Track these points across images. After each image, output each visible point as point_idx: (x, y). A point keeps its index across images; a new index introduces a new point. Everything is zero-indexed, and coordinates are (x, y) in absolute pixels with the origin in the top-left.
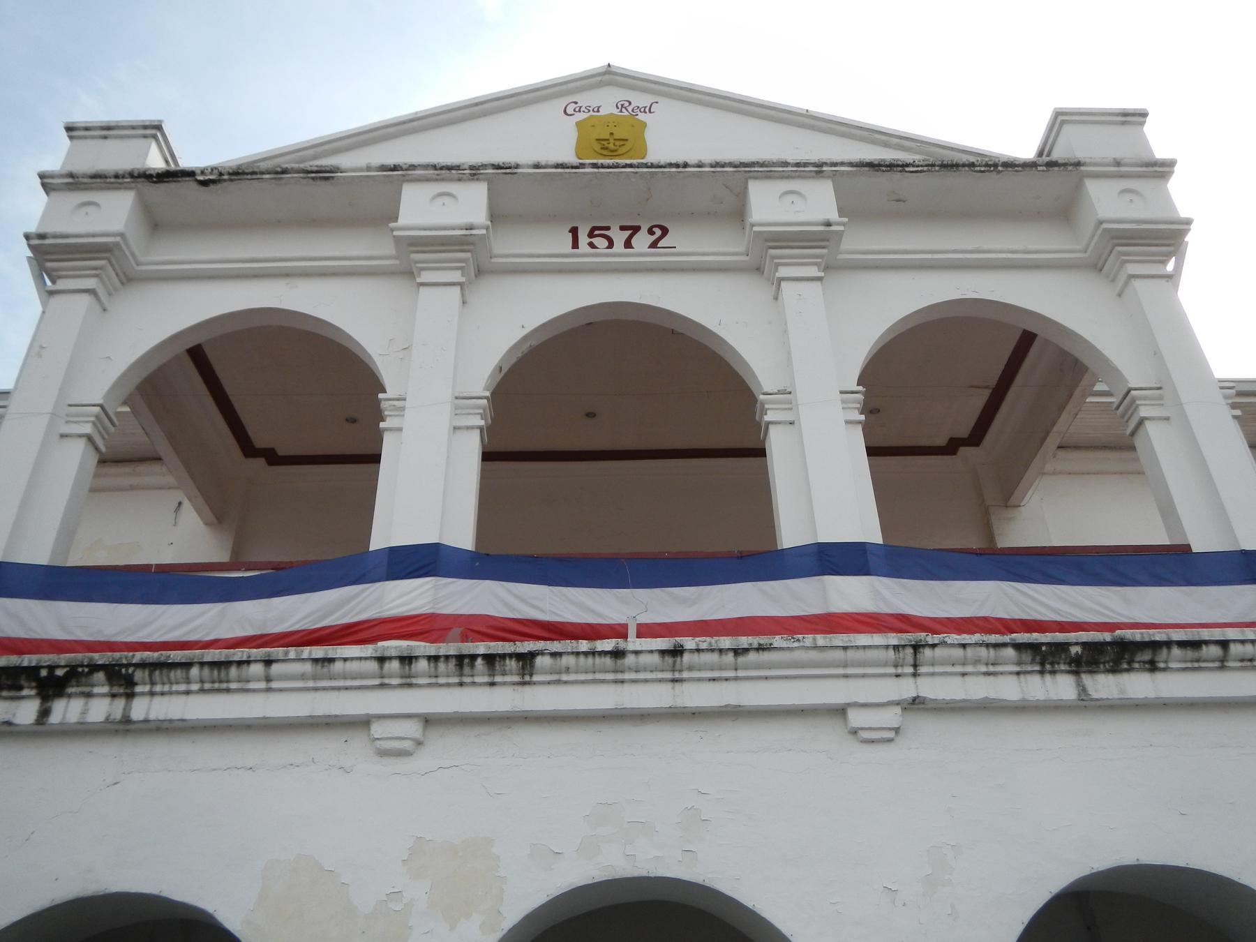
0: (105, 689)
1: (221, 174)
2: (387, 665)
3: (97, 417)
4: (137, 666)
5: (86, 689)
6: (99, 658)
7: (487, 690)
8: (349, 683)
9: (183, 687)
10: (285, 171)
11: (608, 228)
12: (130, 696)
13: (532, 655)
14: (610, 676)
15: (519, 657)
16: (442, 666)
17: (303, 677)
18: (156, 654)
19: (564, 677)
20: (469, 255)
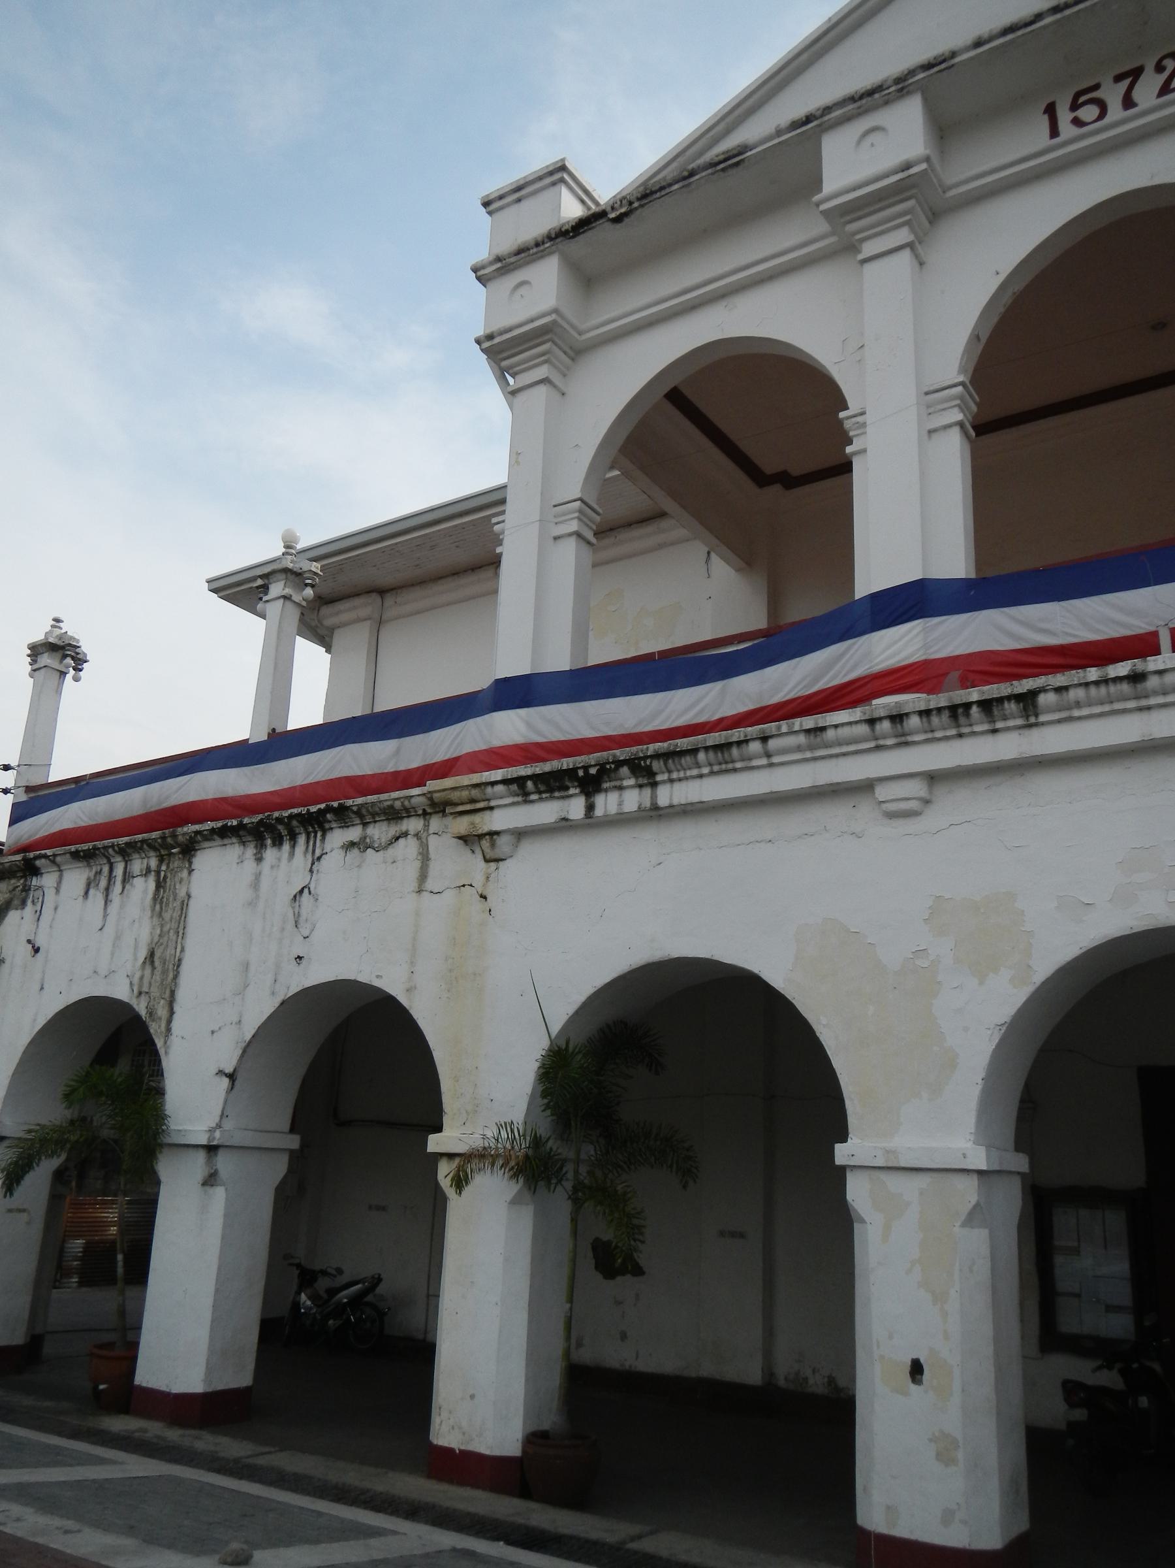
0: (632, 782)
1: (631, 203)
2: (878, 727)
3: (580, 511)
4: (652, 757)
5: (618, 783)
6: (621, 754)
7: (990, 739)
8: (845, 749)
9: (695, 772)
10: (692, 174)
11: (1097, 87)
12: (654, 785)
13: (1033, 694)
14: (1131, 704)
15: (1018, 698)
16: (935, 720)
17: (799, 748)
18: (665, 745)
19: (1076, 713)
20: (912, 203)
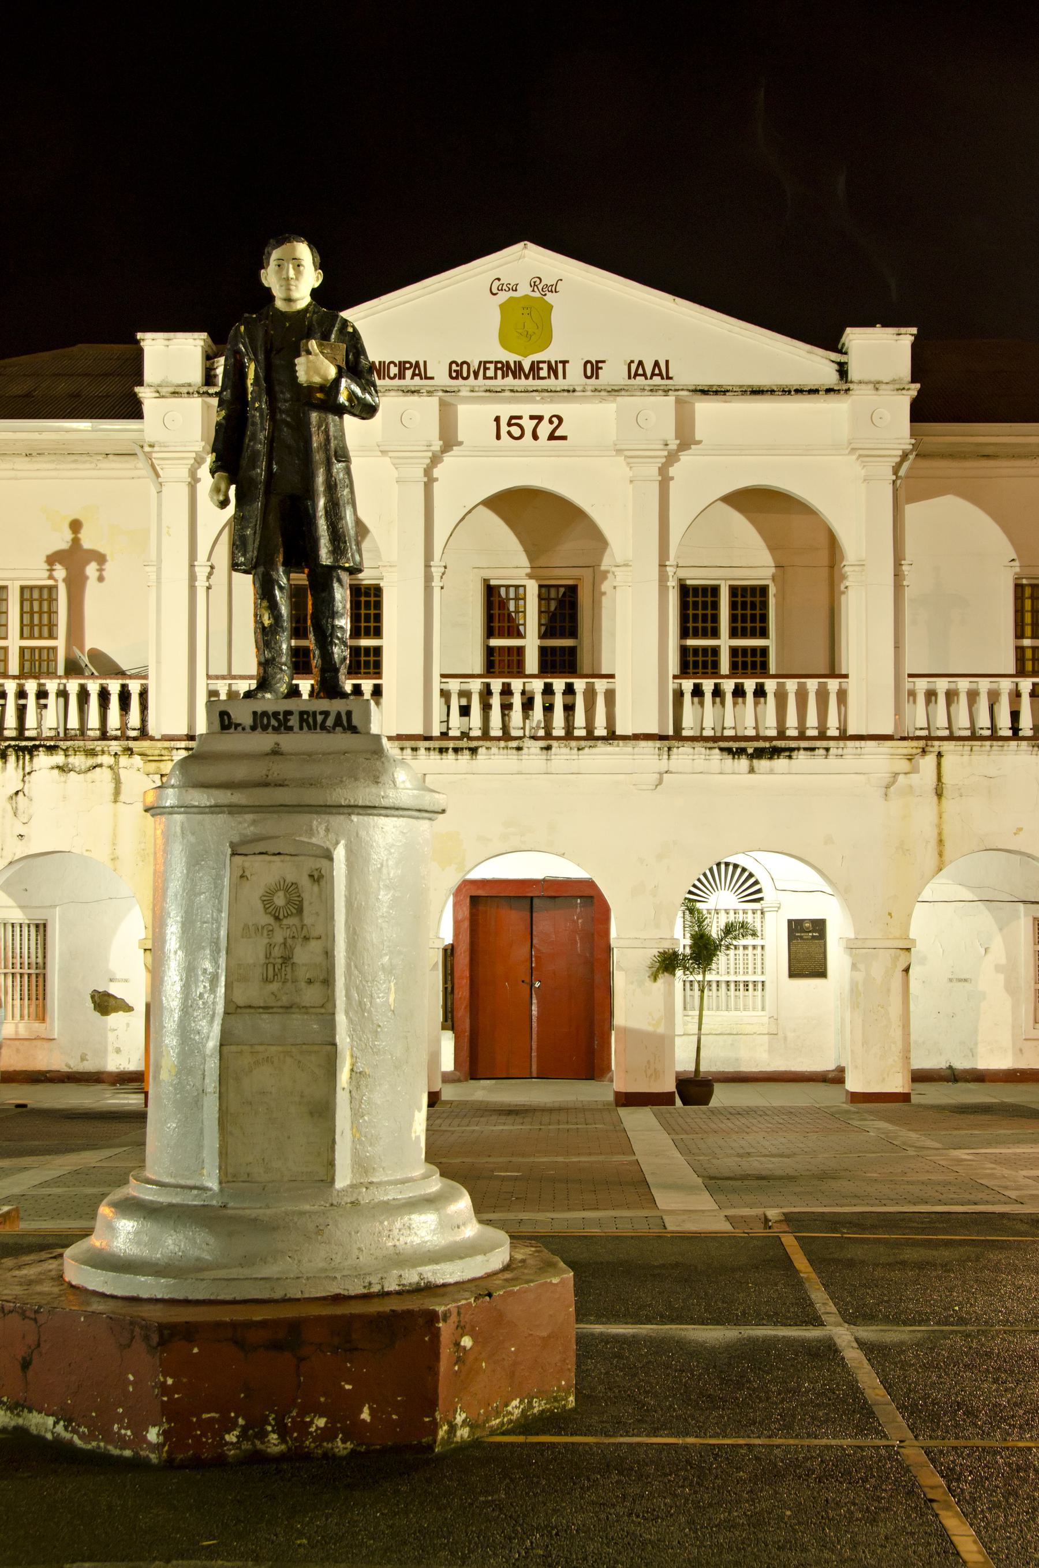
11: (520, 418)
